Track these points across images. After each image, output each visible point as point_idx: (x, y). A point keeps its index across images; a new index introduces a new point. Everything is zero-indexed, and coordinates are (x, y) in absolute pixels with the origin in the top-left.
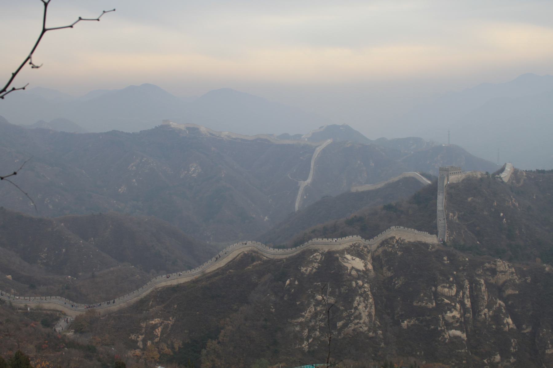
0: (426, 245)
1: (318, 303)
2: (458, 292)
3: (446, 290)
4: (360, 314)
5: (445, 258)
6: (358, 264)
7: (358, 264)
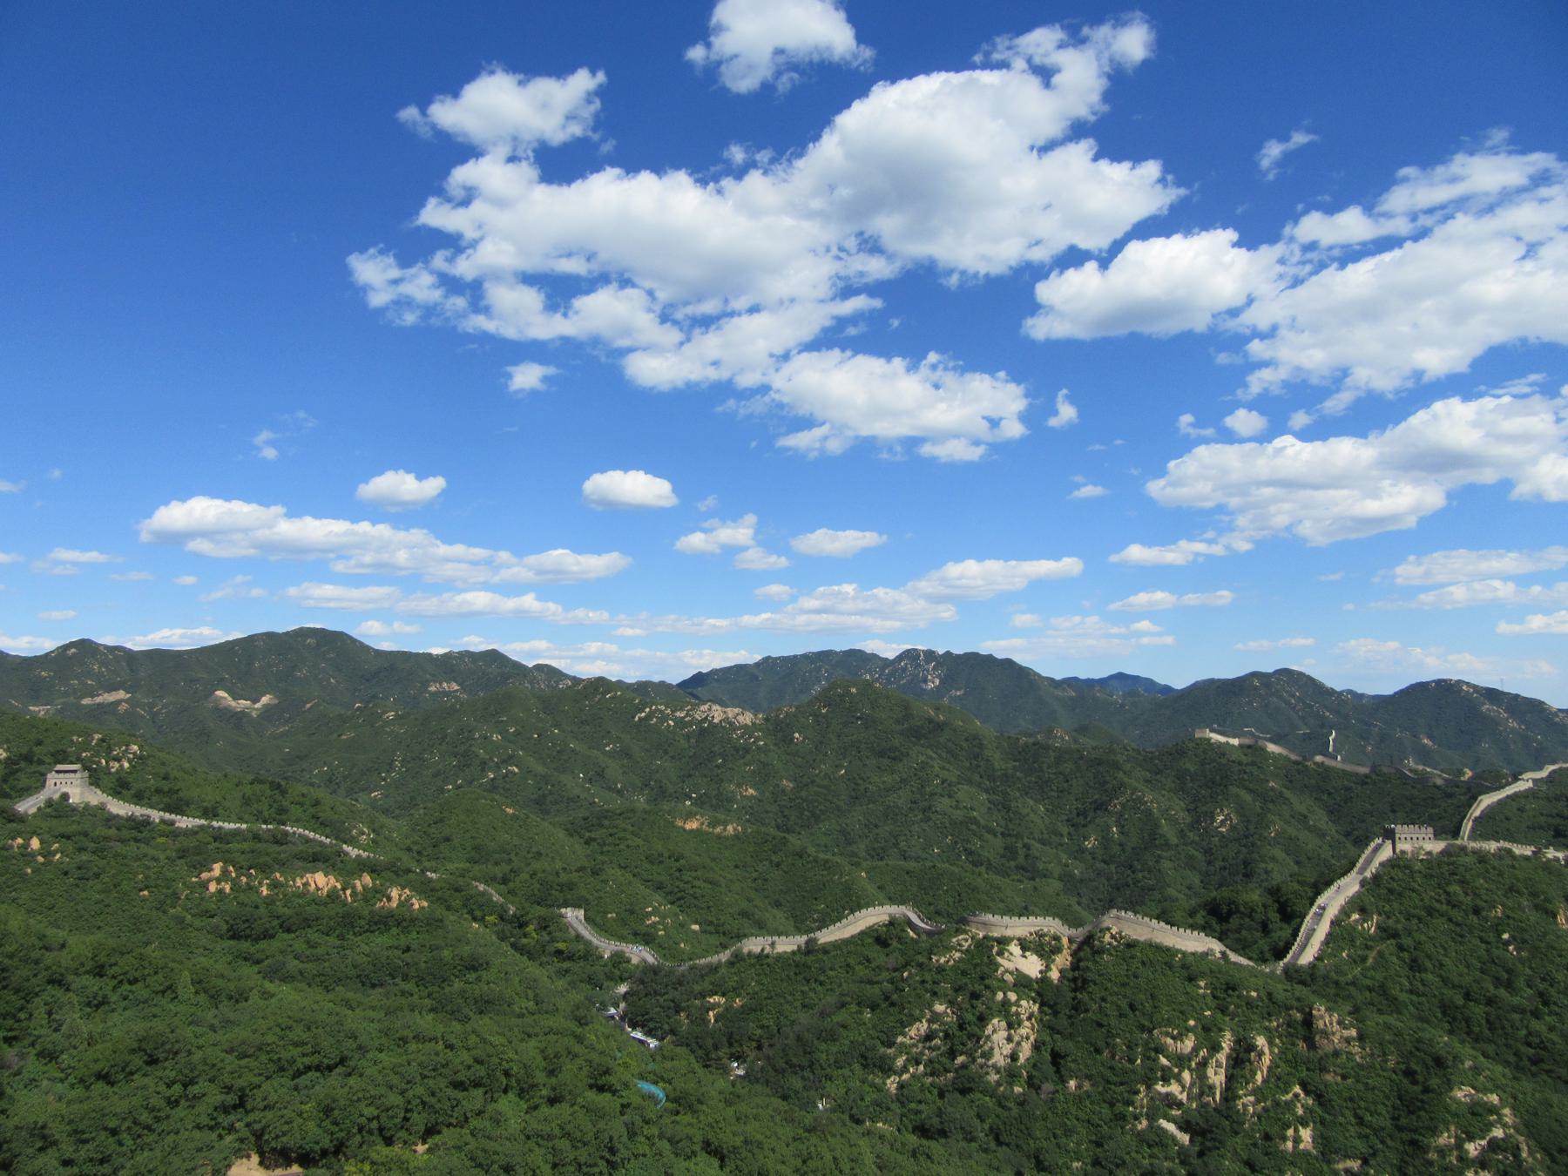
0: (1169, 952)
1: (936, 1017)
2: (1195, 1050)
3: (1169, 1041)
4: (992, 1049)
5: (1202, 984)
6: (1032, 966)
7: (1032, 966)
